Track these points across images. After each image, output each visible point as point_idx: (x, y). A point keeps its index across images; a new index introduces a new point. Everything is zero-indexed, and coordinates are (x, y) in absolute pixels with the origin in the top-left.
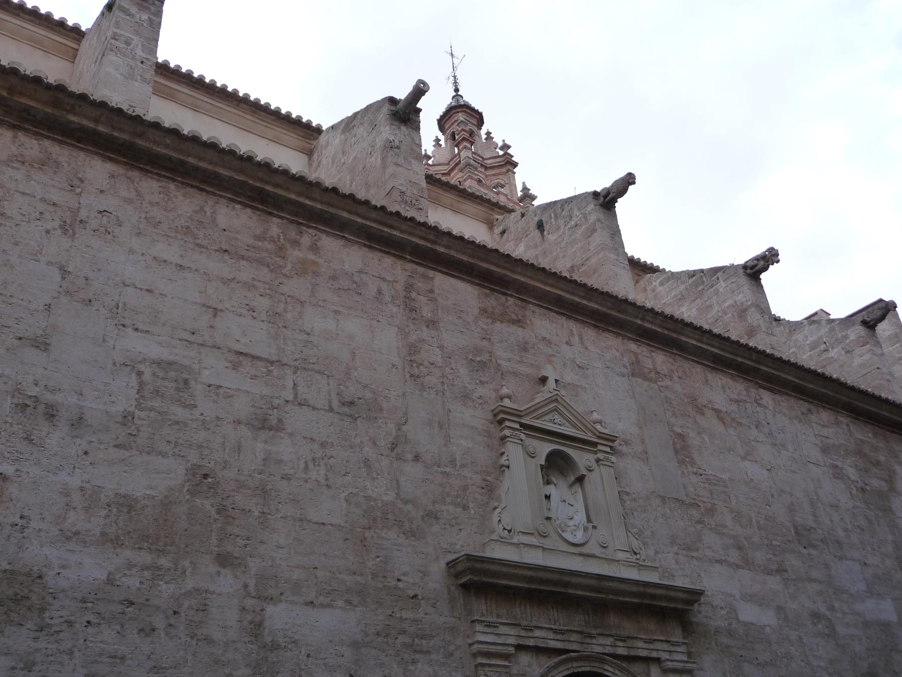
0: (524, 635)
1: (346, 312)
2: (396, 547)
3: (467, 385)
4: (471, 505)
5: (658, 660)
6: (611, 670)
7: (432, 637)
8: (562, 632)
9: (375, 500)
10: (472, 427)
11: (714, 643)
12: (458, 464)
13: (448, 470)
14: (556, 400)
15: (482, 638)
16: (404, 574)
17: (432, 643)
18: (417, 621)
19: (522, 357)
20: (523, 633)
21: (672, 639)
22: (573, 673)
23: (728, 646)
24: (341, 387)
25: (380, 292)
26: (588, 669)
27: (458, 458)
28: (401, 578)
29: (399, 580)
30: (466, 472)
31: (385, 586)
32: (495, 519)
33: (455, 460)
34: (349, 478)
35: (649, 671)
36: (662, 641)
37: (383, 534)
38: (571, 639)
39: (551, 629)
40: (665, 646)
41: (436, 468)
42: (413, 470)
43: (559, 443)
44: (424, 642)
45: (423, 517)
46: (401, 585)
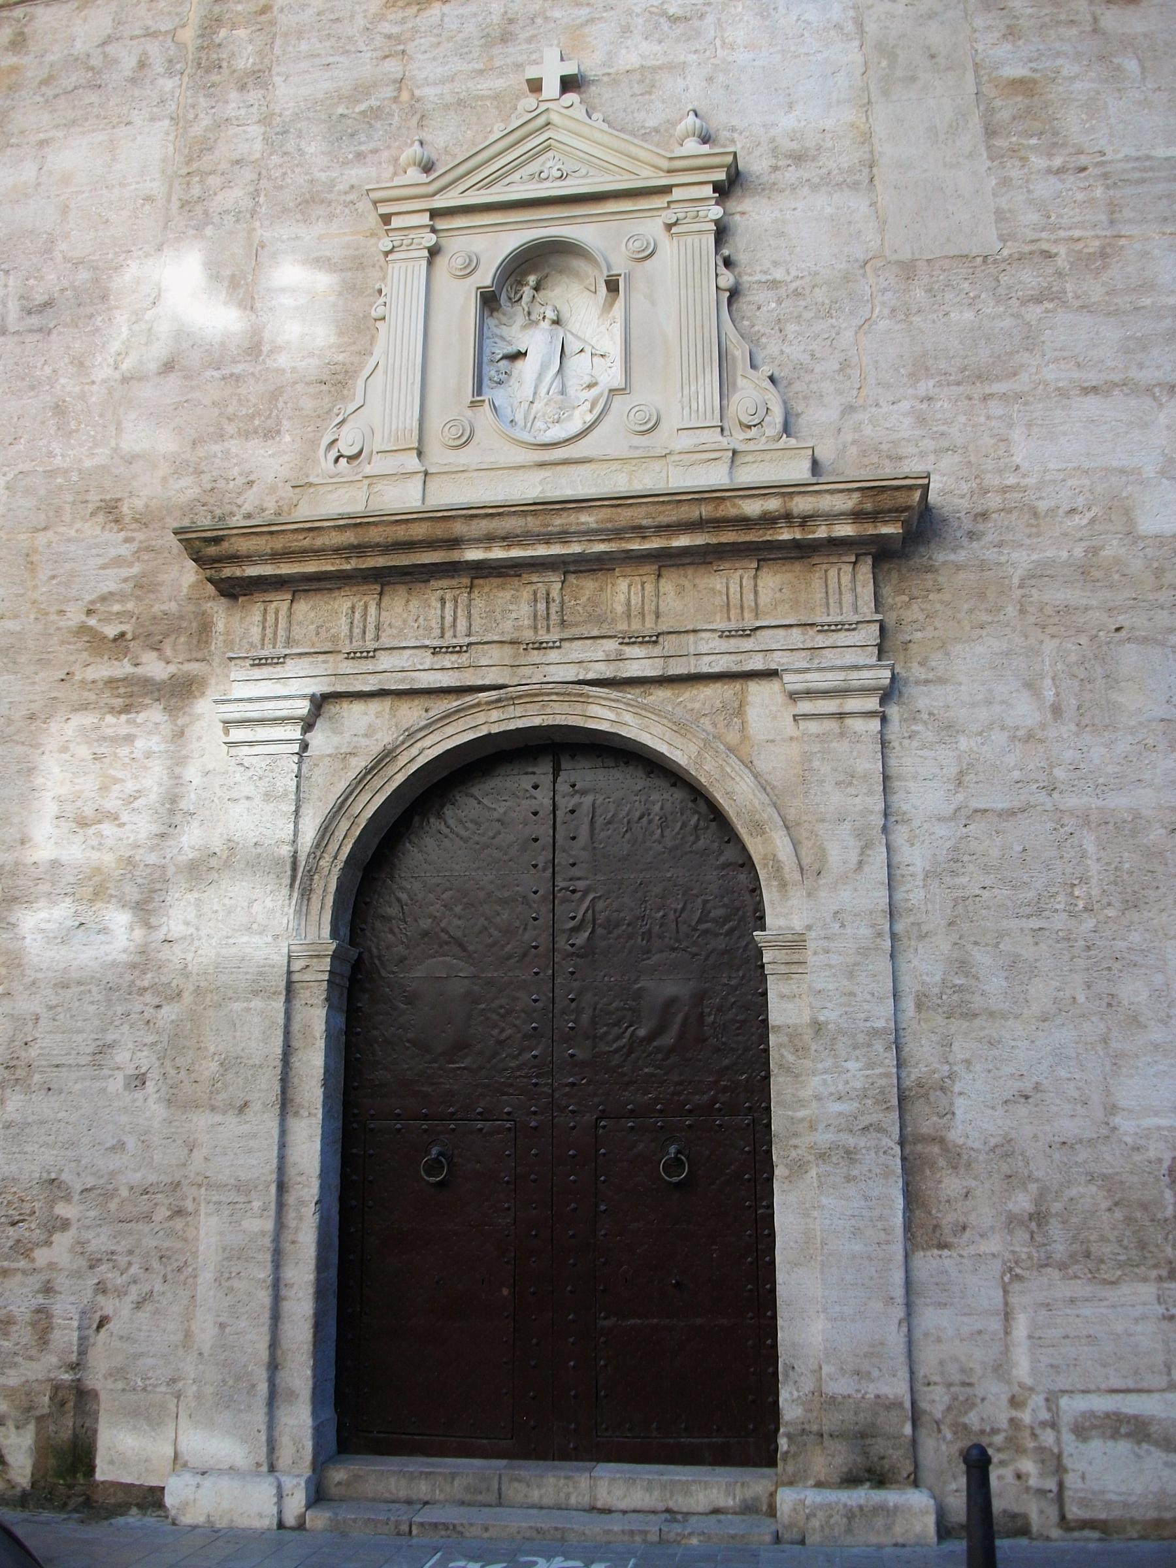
1: (60, 134)
4: (286, 424)
5: (771, 674)
6: (612, 717)
8: (458, 650)
9: (66, 471)
11: (1011, 611)
13: (238, 369)
15: (241, 691)
19: (491, 58)
20: (347, 667)
21: (818, 620)
22: (490, 735)
23: (1067, 610)
24: (32, 282)
25: (142, 65)
26: (537, 721)
31: (59, 629)
34: (21, 446)
36: (791, 626)
37: (73, 533)
38: (484, 662)
39: (427, 647)
40: (796, 637)
41: (209, 373)
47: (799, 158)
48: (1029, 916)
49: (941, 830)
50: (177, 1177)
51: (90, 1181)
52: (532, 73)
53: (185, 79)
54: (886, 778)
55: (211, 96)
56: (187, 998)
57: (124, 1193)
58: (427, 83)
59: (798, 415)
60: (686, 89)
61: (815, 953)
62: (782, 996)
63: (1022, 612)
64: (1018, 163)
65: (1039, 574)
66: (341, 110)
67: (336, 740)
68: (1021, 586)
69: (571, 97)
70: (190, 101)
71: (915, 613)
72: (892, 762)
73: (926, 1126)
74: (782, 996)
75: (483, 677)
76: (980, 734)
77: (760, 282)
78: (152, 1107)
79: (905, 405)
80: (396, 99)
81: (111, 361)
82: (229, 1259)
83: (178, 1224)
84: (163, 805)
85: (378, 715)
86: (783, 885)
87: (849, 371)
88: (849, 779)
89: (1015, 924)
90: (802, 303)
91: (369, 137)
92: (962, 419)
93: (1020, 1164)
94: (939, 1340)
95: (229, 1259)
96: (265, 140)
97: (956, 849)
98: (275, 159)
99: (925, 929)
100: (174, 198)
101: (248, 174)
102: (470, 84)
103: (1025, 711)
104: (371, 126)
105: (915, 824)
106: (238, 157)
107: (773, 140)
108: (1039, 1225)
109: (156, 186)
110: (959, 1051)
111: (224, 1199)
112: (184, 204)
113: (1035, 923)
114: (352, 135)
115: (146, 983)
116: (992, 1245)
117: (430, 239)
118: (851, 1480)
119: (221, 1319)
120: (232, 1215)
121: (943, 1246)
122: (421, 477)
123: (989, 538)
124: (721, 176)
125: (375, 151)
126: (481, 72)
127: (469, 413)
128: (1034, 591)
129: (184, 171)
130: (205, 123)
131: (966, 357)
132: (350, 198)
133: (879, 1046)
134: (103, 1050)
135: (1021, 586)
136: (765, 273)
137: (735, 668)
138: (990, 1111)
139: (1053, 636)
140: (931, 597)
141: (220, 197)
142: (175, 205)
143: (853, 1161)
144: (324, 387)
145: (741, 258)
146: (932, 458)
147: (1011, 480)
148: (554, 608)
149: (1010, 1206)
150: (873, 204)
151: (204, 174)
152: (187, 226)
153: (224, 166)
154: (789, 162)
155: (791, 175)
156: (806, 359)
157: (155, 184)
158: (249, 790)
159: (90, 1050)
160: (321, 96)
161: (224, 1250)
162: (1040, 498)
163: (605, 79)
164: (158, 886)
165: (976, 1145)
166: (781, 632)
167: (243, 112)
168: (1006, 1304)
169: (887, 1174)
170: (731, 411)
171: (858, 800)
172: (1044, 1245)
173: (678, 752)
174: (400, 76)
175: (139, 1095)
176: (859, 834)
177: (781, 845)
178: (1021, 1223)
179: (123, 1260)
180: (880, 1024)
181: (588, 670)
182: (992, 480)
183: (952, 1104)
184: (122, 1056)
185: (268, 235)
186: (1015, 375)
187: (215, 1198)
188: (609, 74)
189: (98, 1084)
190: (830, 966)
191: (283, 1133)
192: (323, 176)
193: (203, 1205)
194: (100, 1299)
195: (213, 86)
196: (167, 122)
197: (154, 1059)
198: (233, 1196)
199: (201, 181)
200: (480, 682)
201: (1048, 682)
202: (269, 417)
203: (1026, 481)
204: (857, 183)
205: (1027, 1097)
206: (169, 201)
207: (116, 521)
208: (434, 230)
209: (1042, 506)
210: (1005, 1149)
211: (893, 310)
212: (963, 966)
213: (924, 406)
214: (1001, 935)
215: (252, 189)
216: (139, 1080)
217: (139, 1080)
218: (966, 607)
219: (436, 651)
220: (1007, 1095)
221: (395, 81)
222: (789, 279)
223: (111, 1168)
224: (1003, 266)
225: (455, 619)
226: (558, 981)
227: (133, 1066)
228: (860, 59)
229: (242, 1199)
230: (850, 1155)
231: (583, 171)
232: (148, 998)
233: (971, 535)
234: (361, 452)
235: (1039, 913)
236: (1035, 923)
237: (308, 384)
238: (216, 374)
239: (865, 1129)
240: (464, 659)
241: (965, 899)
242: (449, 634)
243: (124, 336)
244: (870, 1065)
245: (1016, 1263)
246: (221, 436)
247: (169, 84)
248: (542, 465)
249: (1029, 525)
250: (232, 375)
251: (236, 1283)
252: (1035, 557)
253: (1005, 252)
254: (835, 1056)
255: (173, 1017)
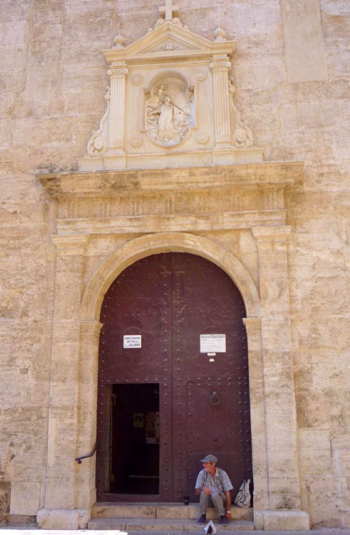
0: (101, 226)
2: (4, 181)
3: (83, 44)
4: (74, 137)
6: (193, 243)
7: (24, 238)
10: (84, 76)
11: (331, 208)
12: (66, 108)
13: (56, 116)
14: (168, 29)
16: (8, 199)
17: (23, 242)
18: (14, 228)
20: (99, 225)
27: (66, 104)
28: (6, 201)
29: (4, 203)
30: (72, 113)
32: (90, 143)
33: (63, 107)
35: (238, 239)
41: (45, 117)
42: (23, 123)
43: (162, 67)
44: (17, 241)
45: (29, 155)
46: (4, 206)
47: (257, 44)
48: (337, 314)
49: (307, 284)
50: (40, 405)
51: (8, 407)
52: (161, 9)
53: (32, 5)
54: (289, 266)
55: (42, 12)
56: (43, 341)
57: (20, 410)
58: (122, 11)
59: (257, 138)
60: (217, 17)
61: (264, 326)
62: (253, 341)
63: (335, 208)
64: (334, 47)
65: (342, 195)
66: (91, 20)
67: (95, 250)
68: (335, 199)
69: (176, 20)
70: (34, 13)
71: (298, 209)
72: (290, 260)
73: (303, 386)
74: (253, 341)
75: (148, 229)
76: (320, 250)
77: (243, 90)
78: (30, 381)
79: (295, 135)
80: (111, 17)
81: (8, 111)
82: (59, 433)
83: (40, 421)
84: (32, 273)
85: (110, 242)
86: (253, 303)
87: (275, 123)
88: (276, 266)
89: (333, 316)
90: (259, 98)
91: (102, 31)
92: (315, 140)
93: (336, 398)
94: (308, 459)
95: (59, 433)
96: (63, 30)
97: (312, 290)
98: (67, 38)
99: (302, 318)
100: (29, 50)
101: (57, 43)
102: (138, 12)
103: (336, 244)
104: (102, 27)
105: (299, 281)
106: (53, 36)
107: (248, 37)
108: (342, 420)
109: (22, 45)
110: (314, 359)
111: (58, 412)
112: (33, 53)
113: (340, 316)
114: (95, 30)
115: (27, 336)
116: (327, 426)
117: (126, 71)
118: (279, 508)
119: (57, 455)
120: (60, 418)
121: (309, 426)
122: (125, 158)
123: (324, 182)
124: (230, 51)
125: (104, 36)
126: (142, 8)
127: (141, 135)
128: (339, 201)
129: (32, 40)
130: (40, 22)
131: (316, 118)
132: (96, 53)
133: (287, 358)
134: (11, 361)
135: (335, 199)
136: (246, 86)
137: (236, 228)
138: (324, 380)
139: (346, 217)
140: (304, 203)
141: (46, 51)
142: (30, 54)
143: (278, 397)
144: (87, 124)
145: (238, 81)
146: (304, 154)
147: (331, 162)
148: (173, 206)
149: (332, 413)
150: (284, 62)
151: (41, 42)
152: (35, 61)
153: (48, 39)
154: (254, 45)
155: (254, 50)
156: (260, 118)
157: (22, 45)
158: (64, 268)
159: (7, 360)
160: (83, 14)
161: (58, 430)
162: (342, 169)
163: (188, 12)
164: (31, 302)
165: (320, 392)
166: (252, 215)
167: (54, 19)
168: (331, 446)
169: (290, 401)
170: (234, 136)
171: (279, 274)
172: (344, 426)
173: (217, 257)
174: (112, 8)
175: (25, 376)
176: (279, 285)
177: (253, 289)
178: (336, 419)
179: (20, 435)
180: (287, 350)
181: (185, 227)
182: (325, 162)
183: (312, 378)
184: (19, 362)
185: (65, 66)
186: (333, 124)
187: (54, 412)
188: (189, 10)
189: (10, 372)
190: (270, 330)
191: (79, 388)
192: (85, 45)
193: (50, 414)
194: (12, 448)
195: (42, 8)
196: (25, 21)
197: (30, 363)
198: (60, 411)
199: (40, 45)
200: (147, 231)
201: (344, 233)
202: (68, 134)
203: (336, 163)
204: (278, 54)
205: (337, 376)
206: (28, 51)
207: (12, 170)
208: (127, 68)
209: (342, 172)
210: (329, 393)
211: (291, 101)
212: (315, 330)
213: (301, 135)
214: (328, 320)
215: (58, 48)
216: (25, 371)
217: (25, 371)
218: (316, 207)
219: (131, 220)
220: (331, 375)
221: (111, 10)
222: (254, 89)
223: (15, 402)
224: (330, 85)
225: (138, 208)
226: (173, 335)
227: (23, 365)
228: (279, 7)
229: (64, 412)
230: (277, 395)
231: (181, 47)
232: (28, 341)
233: (318, 182)
234: (102, 148)
235: (341, 312)
236: (340, 316)
237: (81, 122)
238: (48, 117)
239: (283, 386)
240: (141, 223)
241: (315, 308)
242: (136, 214)
243: (12, 102)
244: (284, 364)
245: (334, 432)
246: (50, 140)
247: (25, 7)
248: (167, 155)
249: (338, 178)
250: (54, 118)
251: (62, 442)
252: (339, 189)
253: (330, 80)
254: (272, 361)
255: (38, 348)
